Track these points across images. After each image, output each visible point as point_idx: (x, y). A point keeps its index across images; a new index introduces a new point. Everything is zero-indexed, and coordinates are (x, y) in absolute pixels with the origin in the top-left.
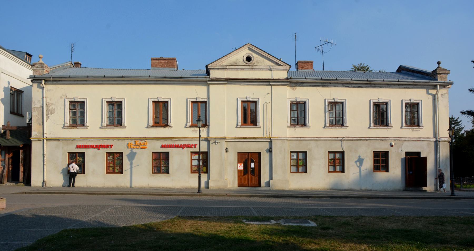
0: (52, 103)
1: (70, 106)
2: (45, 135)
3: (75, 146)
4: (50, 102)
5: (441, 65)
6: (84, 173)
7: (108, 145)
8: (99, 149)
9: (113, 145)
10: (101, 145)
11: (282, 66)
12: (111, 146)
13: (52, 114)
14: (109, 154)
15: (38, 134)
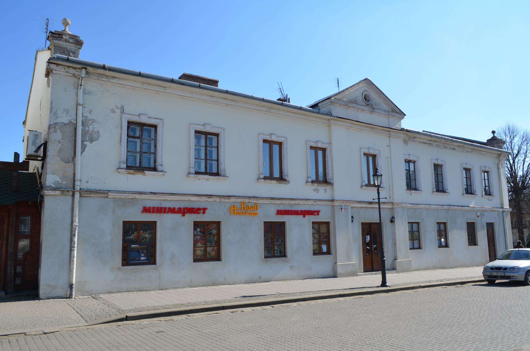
0: (93, 120)
1: (128, 130)
2: (77, 183)
3: (141, 209)
4: (90, 116)
5: (495, 135)
6: (154, 263)
7: (199, 209)
8: (184, 215)
9: (207, 209)
10: (187, 208)
11: (397, 113)
12: (204, 210)
13: (92, 141)
14: (196, 224)
15: (62, 181)
